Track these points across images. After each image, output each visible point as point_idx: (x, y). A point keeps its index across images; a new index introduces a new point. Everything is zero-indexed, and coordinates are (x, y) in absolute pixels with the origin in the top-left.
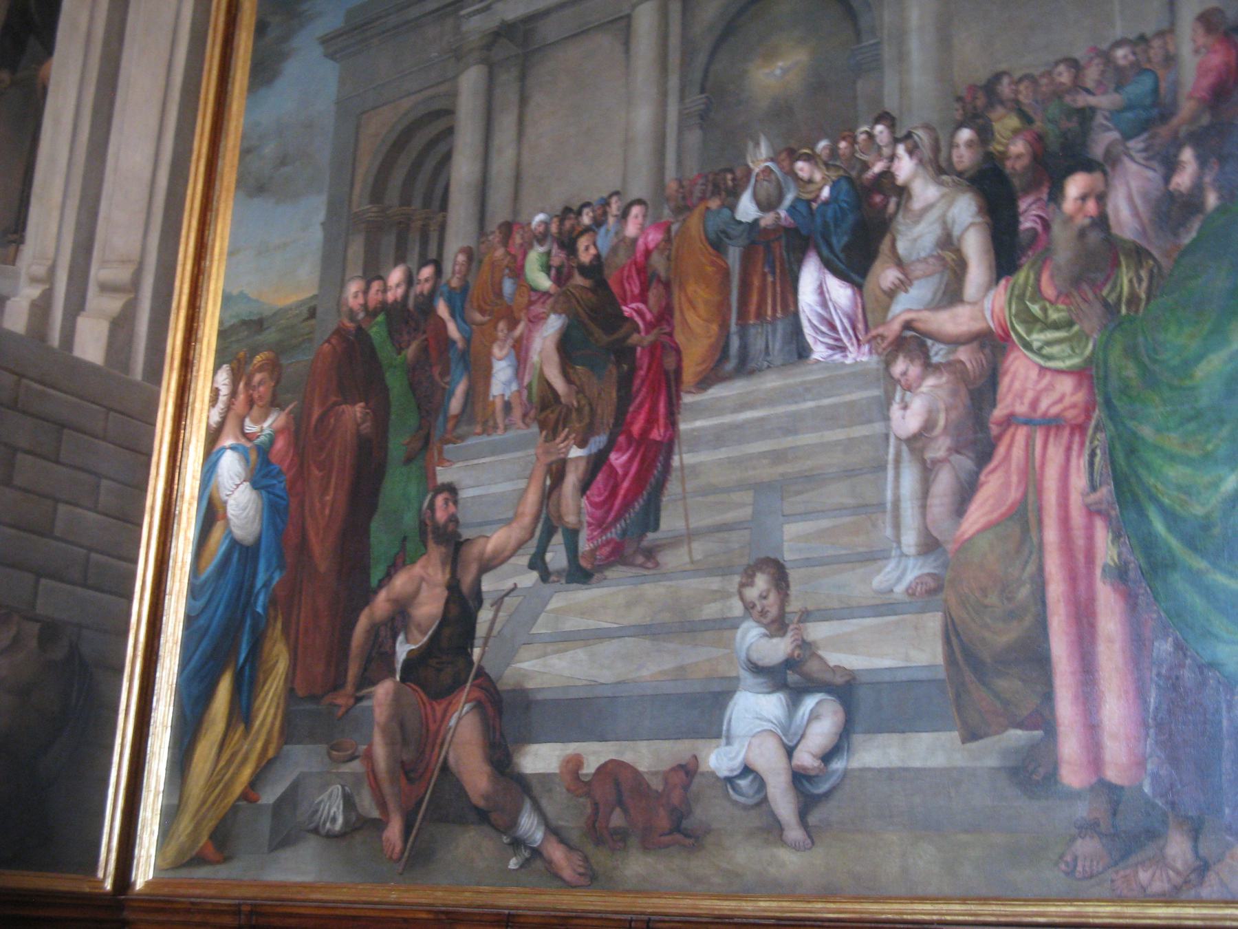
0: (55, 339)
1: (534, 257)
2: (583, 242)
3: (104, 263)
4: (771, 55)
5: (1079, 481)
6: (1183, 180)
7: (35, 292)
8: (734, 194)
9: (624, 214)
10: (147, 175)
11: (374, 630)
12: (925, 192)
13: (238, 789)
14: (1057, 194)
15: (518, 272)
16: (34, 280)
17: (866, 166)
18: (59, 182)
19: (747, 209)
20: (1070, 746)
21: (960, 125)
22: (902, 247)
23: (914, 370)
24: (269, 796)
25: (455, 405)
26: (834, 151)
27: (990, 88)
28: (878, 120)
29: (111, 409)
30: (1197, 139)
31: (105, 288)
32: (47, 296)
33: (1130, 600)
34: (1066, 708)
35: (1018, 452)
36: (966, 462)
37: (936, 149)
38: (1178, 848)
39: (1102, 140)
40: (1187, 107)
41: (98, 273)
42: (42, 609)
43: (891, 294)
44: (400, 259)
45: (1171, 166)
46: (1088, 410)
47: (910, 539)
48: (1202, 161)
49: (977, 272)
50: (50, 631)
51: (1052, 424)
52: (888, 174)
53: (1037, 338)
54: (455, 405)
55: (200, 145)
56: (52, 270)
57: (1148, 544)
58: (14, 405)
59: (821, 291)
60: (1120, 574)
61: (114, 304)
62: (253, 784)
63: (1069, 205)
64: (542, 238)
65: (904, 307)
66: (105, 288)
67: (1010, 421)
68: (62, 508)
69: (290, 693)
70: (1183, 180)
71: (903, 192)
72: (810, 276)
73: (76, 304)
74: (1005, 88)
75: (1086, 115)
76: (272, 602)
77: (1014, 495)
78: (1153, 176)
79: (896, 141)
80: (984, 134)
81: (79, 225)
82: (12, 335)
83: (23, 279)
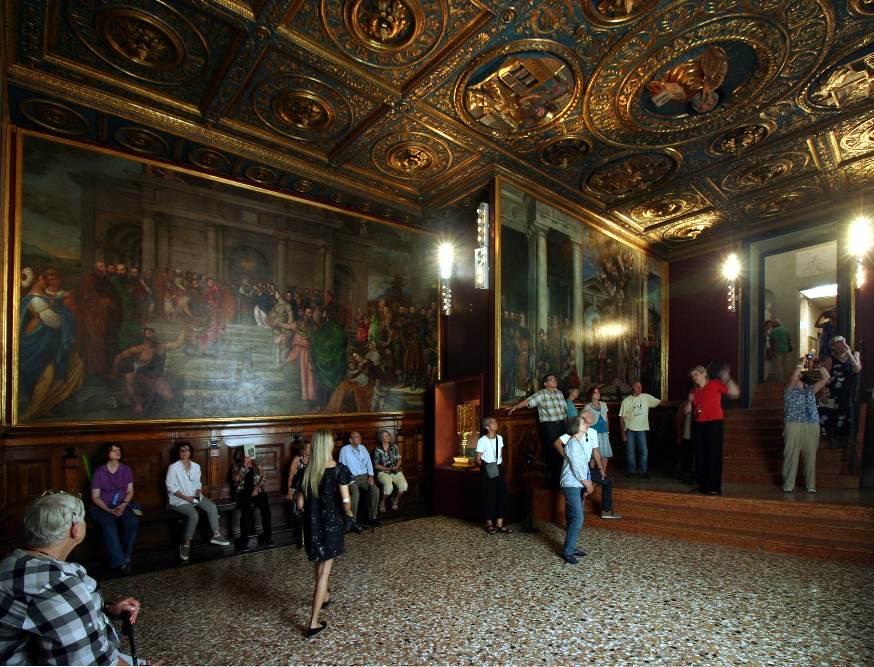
1: (177, 281)
2: (194, 282)
4: (247, 260)
5: (306, 356)
6: (324, 315)
8: (238, 287)
9: (207, 279)
12: (281, 302)
14: (305, 311)
15: (172, 282)
17: (269, 293)
19: (241, 291)
20: (304, 394)
21: (288, 292)
22: (276, 310)
23: (278, 333)
25: (151, 308)
26: (262, 287)
27: (295, 287)
28: (273, 284)
30: (326, 310)
33: (314, 375)
34: (304, 389)
35: (297, 350)
36: (288, 350)
37: (284, 294)
38: (319, 408)
39: (313, 305)
40: (325, 305)
43: (275, 318)
45: (322, 313)
46: (308, 346)
47: (277, 360)
48: (327, 313)
49: (291, 319)
51: (303, 347)
52: (273, 296)
53: (301, 333)
54: (151, 308)
57: (316, 367)
59: (259, 313)
60: (312, 371)
63: (307, 313)
64: (180, 276)
65: (276, 320)
67: (296, 345)
70: (324, 315)
71: (277, 300)
72: (257, 310)
74: (296, 289)
75: (310, 299)
77: (296, 356)
78: (320, 313)
79: (276, 290)
80: (292, 296)
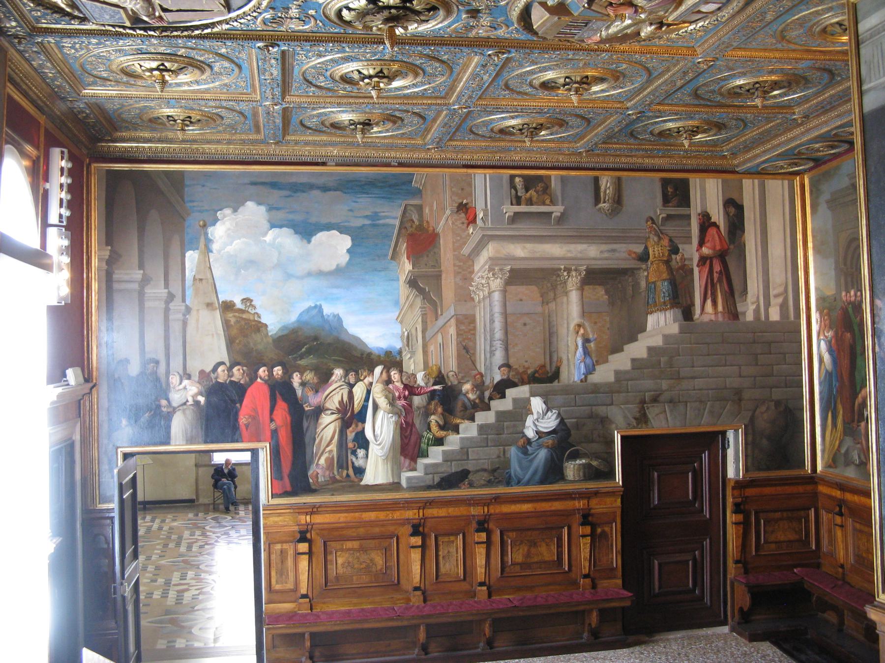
0: (763, 318)
3: (774, 289)
7: (754, 307)
10: (784, 254)
11: (859, 405)
13: (836, 447)
16: (753, 303)
18: (755, 269)
24: (843, 451)
29: (784, 333)
31: (776, 296)
32: (758, 306)
41: (772, 292)
42: (774, 397)
44: (853, 288)
50: (778, 403)
55: (800, 236)
56: (758, 297)
58: (754, 342)
61: (780, 300)
62: (839, 446)
66: (776, 296)
68: (774, 367)
69: (844, 420)
73: (768, 304)
76: (837, 391)
81: (763, 281)
82: (749, 321)
83: (749, 304)
